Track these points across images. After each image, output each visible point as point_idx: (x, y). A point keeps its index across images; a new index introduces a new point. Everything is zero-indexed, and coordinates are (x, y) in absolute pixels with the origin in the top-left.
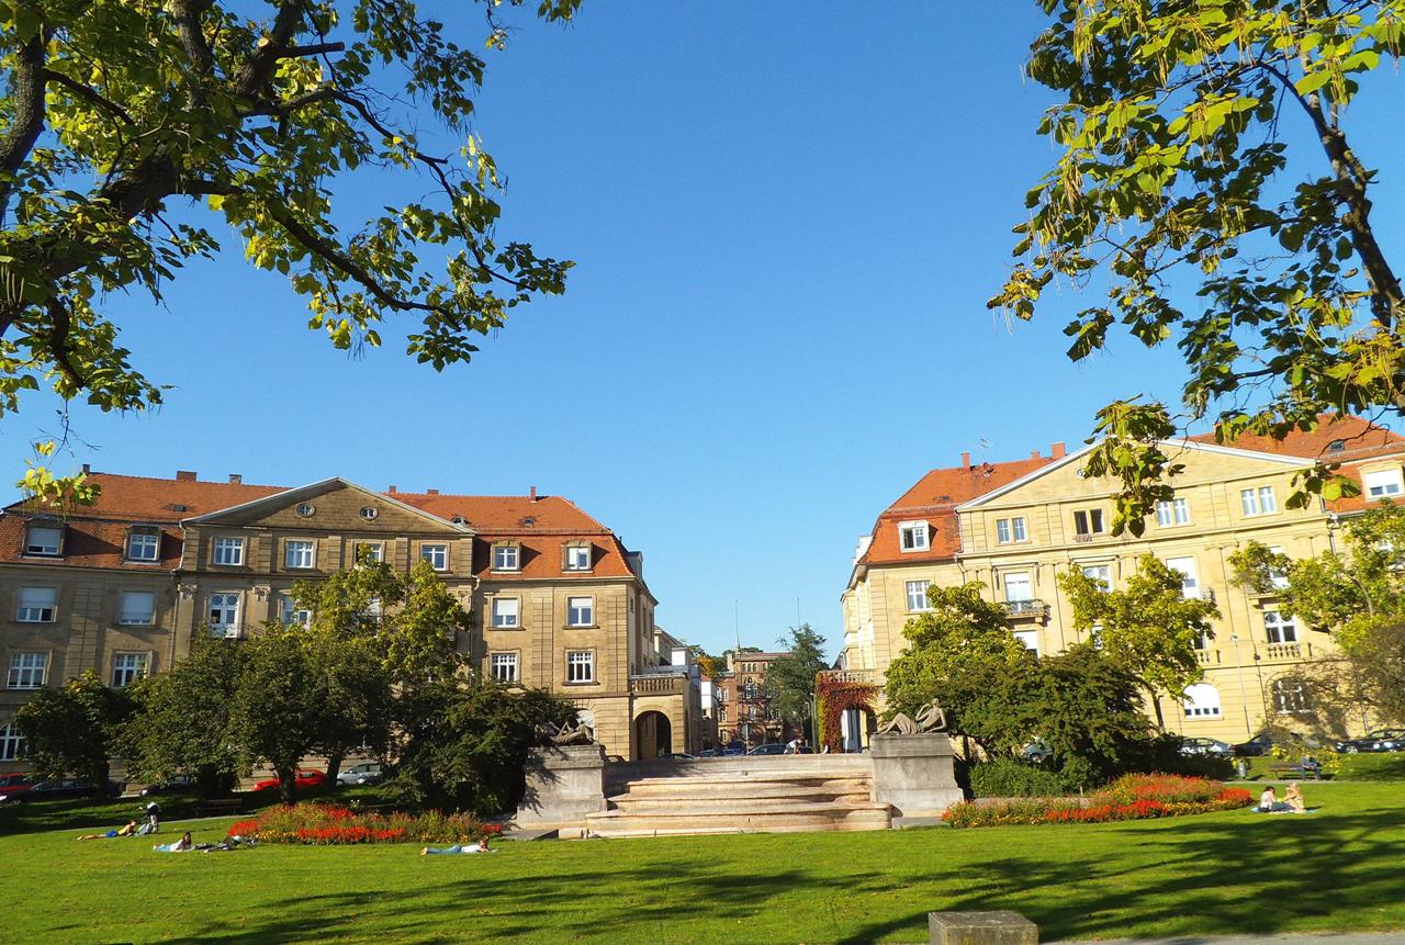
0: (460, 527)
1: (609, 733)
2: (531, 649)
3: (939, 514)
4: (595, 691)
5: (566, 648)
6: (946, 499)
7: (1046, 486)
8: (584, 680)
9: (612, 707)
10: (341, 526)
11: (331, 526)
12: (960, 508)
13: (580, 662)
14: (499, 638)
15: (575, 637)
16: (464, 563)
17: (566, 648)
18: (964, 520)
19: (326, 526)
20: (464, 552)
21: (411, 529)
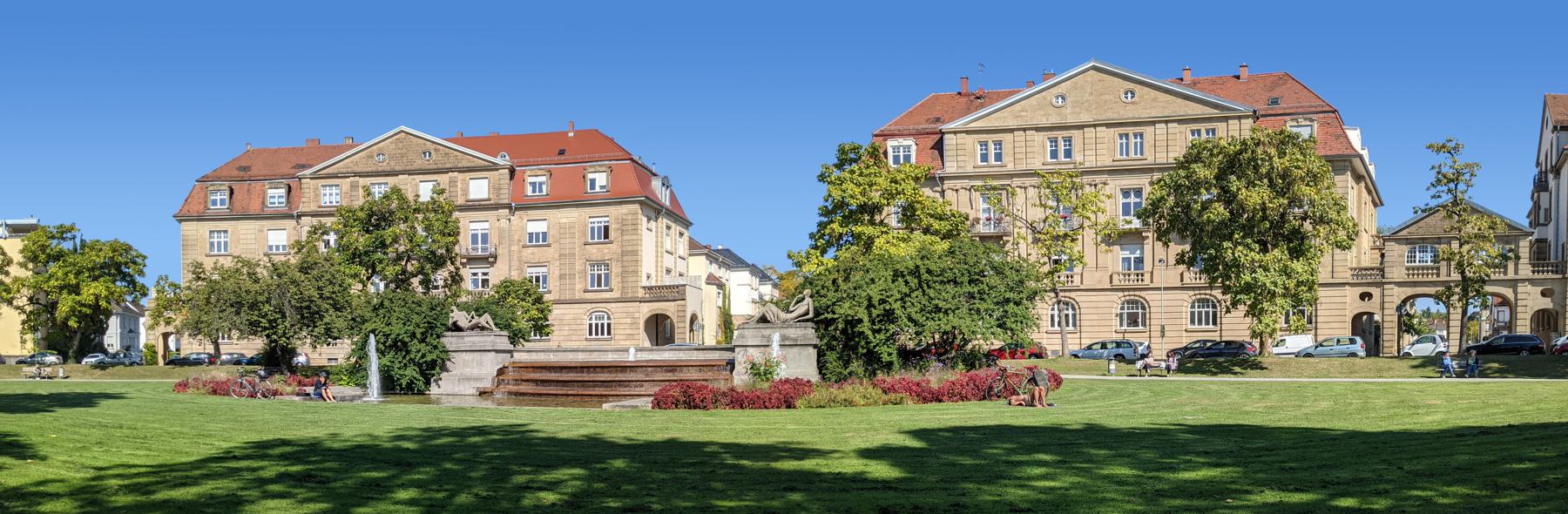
0: (498, 160)
1: (622, 332)
2: (558, 262)
3: (927, 134)
4: (613, 297)
5: (587, 260)
6: (938, 120)
7: (1027, 111)
8: (603, 288)
9: (626, 310)
10: (408, 168)
11: (400, 168)
12: (945, 127)
13: (600, 272)
14: (533, 254)
15: (595, 251)
16: (502, 191)
17: (587, 260)
18: (949, 140)
19: (397, 168)
20: (502, 182)
21: (460, 165)
